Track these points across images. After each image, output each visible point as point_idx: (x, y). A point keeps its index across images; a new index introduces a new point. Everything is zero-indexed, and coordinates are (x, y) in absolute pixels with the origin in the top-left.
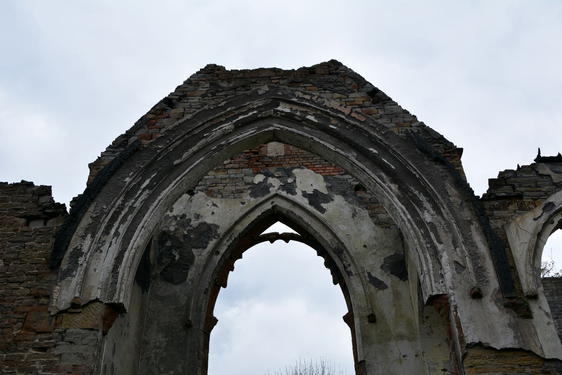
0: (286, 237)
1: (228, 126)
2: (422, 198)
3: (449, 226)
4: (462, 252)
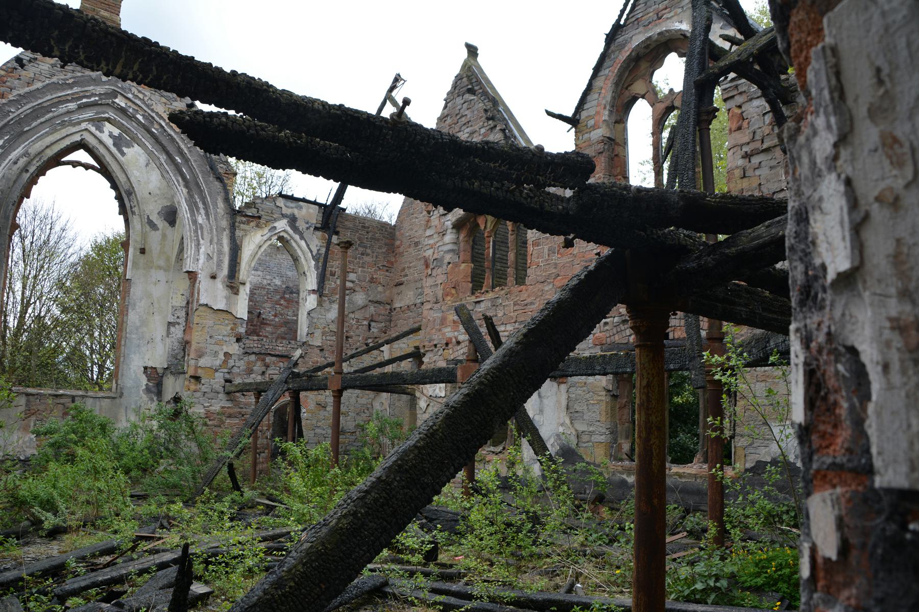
0: (87, 167)
1: (72, 106)
2: (201, 205)
3: (211, 230)
4: (214, 249)
